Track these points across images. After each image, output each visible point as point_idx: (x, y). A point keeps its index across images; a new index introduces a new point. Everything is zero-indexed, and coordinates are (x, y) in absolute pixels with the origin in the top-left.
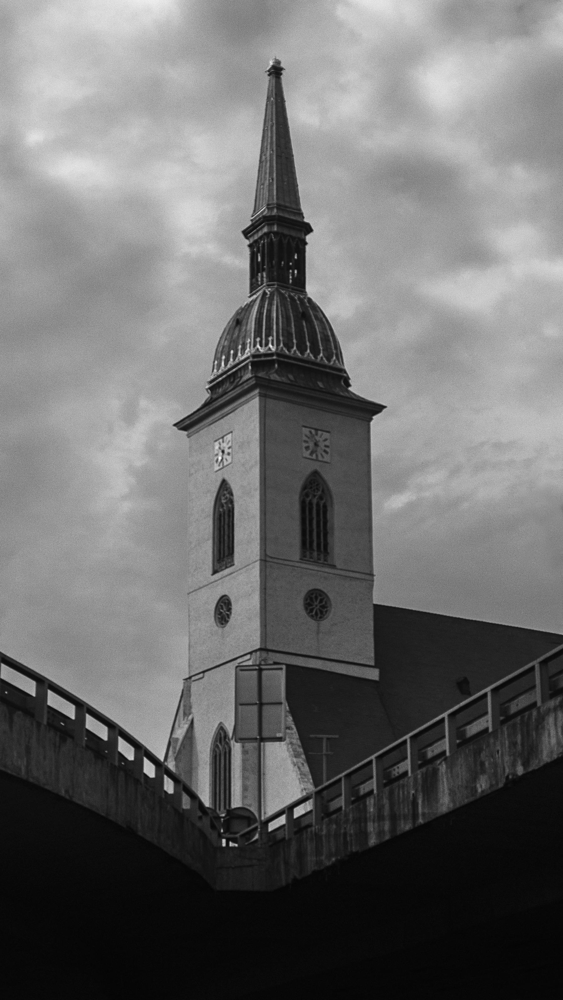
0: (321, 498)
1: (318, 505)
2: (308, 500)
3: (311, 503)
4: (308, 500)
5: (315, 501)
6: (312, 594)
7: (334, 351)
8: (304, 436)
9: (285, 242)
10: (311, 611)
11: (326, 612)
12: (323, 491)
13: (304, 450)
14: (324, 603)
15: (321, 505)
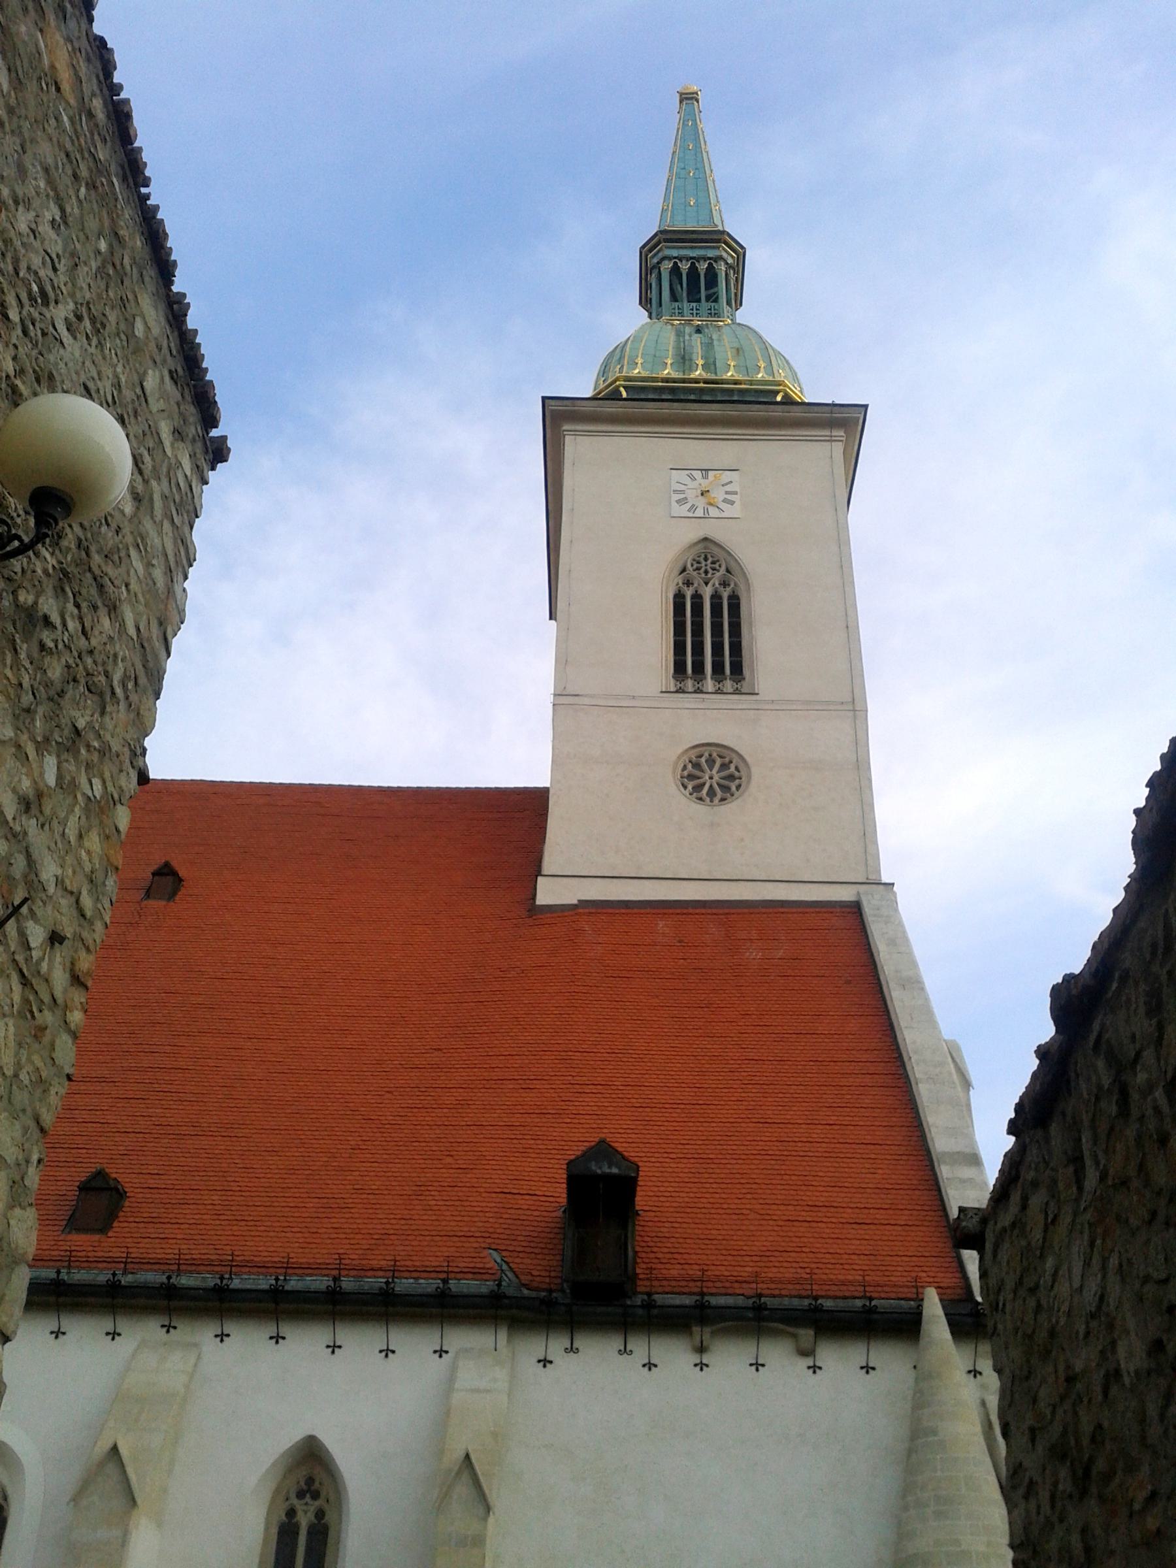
0: (725, 584)
1: (716, 598)
2: (689, 593)
3: (697, 598)
4: (689, 593)
5: (707, 592)
6: (701, 756)
7: (762, 364)
8: (673, 483)
9: (685, 267)
10: (698, 788)
11: (738, 787)
12: (728, 571)
13: (674, 504)
14: (732, 768)
15: (725, 596)
